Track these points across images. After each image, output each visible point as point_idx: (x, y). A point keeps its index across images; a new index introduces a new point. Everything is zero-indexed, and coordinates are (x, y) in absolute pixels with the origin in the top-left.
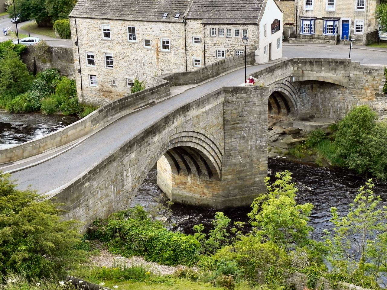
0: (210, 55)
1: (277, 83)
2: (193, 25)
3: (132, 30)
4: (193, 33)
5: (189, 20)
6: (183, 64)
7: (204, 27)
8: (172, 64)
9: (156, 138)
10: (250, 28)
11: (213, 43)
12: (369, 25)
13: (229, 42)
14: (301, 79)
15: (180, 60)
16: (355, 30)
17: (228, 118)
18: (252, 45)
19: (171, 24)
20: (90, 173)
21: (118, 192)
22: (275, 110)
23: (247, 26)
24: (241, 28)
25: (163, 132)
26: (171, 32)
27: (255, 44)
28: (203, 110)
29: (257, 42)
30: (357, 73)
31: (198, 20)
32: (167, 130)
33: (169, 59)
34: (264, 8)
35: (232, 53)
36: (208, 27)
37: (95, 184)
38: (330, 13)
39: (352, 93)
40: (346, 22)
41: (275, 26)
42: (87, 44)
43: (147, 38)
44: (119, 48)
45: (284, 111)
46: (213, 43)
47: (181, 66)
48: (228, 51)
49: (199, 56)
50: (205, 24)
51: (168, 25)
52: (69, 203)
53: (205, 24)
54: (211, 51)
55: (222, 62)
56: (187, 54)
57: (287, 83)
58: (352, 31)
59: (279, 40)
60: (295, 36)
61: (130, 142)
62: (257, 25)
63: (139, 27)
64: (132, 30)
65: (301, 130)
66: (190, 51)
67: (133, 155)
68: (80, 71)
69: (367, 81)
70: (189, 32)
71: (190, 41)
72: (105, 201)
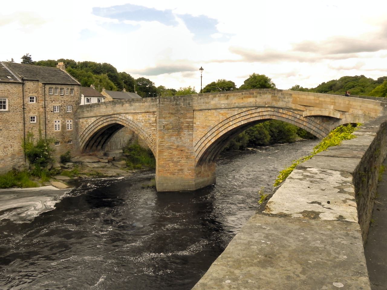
0: (49, 111)
4: (29, 93)
5: (27, 81)
6: (21, 121)
7: (44, 86)
8: (10, 122)
11: (51, 100)
13: (62, 99)
18: (77, 101)
19: (9, 84)
23: (74, 86)
26: (9, 92)
27: (78, 100)
31: (33, 81)
33: (8, 118)
35: (64, 108)
36: (47, 87)
46: (51, 100)
47: (20, 124)
48: (62, 106)
49: (35, 113)
50: (45, 84)
51: (6, 85)
53: (45, 84)
56: (25, 112)
65: (115, 157)
66: (27, 109)
70: (26, 92)
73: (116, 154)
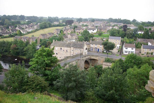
1: (86, 59)
2: (72, 48)
3: (61, 48)
15: (69, 54)
22: (86, 64)
24: (80, 49)
38: (96, 47)
40: (98, 49)
41: (86, 49)
44: (59, 51)
54: (75, 52)
55: (77, 55)
60: (89, 51)
63: (62, 48)
64: (61, 48)
71: (71, 51)
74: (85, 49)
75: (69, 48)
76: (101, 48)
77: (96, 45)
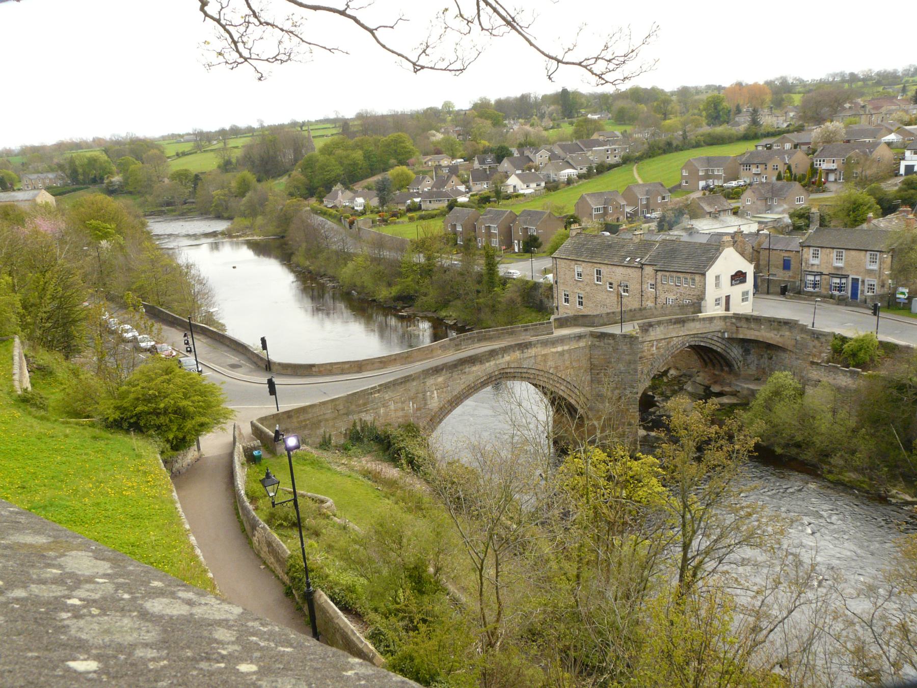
2: (649, 270)
3: (599, 272)
9: (474, 369)
10: (697, 278)
12: (883, 286)
14: (734, 336)
16: (866, 290)
17: (596, 362)
20: (379, 386)
21: (418, 409)
25: (487, 364)
28: (554, 350)
29: (703, 292)
30: (804, 336)
32: (492, 363)
34: (717, 258)
36: (659, 273)
37: (387, 397)
38: (838, 268)
39: (798, 359)
40: (855, 281)
42: (563, 283)
43: (610, 281)
44: (588, 289)
45: (726, 369)
50: (657, 271)
52: (354, 407)
53: (657, 271)
57: (715, 338)
58: (863, 291)
59: (745, 294)
61: (437, 367)
62: (704, 275)
63: (604, 270)
64: (599, 272)
67: (440, 379)
68: (557, 308)
69: (814, 347)
72: (400, 414)
73: (743, 388)
74: (726, 280)
75: (634, 274)
76: (870, 272)
77: (839, 257)
